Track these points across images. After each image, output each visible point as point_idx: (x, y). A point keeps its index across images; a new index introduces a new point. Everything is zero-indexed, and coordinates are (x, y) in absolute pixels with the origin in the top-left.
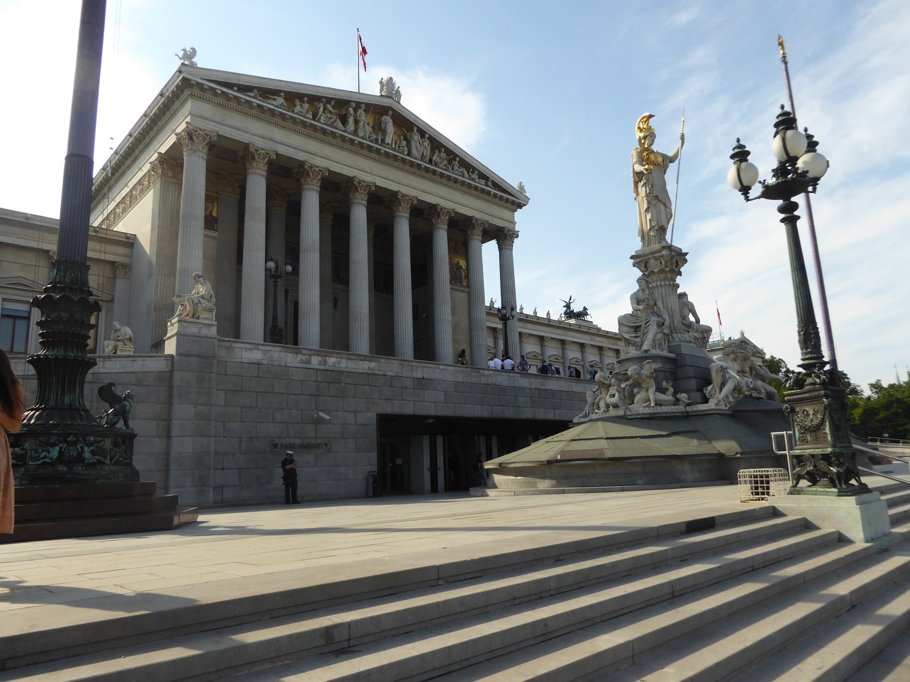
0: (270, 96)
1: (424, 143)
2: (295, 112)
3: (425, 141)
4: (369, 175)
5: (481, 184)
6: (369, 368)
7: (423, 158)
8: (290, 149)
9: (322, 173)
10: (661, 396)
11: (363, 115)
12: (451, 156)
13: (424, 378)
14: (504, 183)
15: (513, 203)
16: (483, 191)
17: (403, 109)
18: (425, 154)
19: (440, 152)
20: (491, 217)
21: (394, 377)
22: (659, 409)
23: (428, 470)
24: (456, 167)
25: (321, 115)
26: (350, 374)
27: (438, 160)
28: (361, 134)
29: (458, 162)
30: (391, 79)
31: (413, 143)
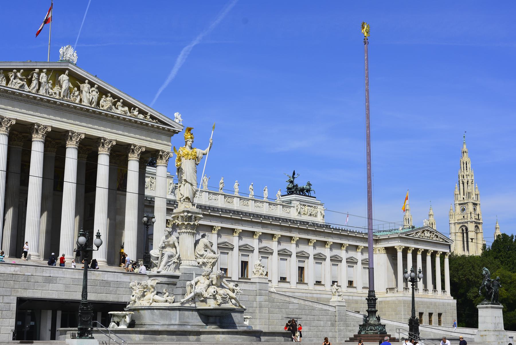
1: (93, 92)
3: (94, 91)
6: (14, 271)
7: (91, 103)
9: (11, 123)
10: (157, 297)
11: (44, 78)
12: (116, 100)
13: (50, 277)
15: (169, 130)
16: (141, 123)
18: (93, 101)
19: (107, 96)
21: (30, 276)
22: (154, 304)
23: (50, 330)
24: (120, 108)
25: (13, 81)
26: (2, 274)
27: (104, 104)
28: (42, 91)
29: (122, 103)
31: (84, 92)
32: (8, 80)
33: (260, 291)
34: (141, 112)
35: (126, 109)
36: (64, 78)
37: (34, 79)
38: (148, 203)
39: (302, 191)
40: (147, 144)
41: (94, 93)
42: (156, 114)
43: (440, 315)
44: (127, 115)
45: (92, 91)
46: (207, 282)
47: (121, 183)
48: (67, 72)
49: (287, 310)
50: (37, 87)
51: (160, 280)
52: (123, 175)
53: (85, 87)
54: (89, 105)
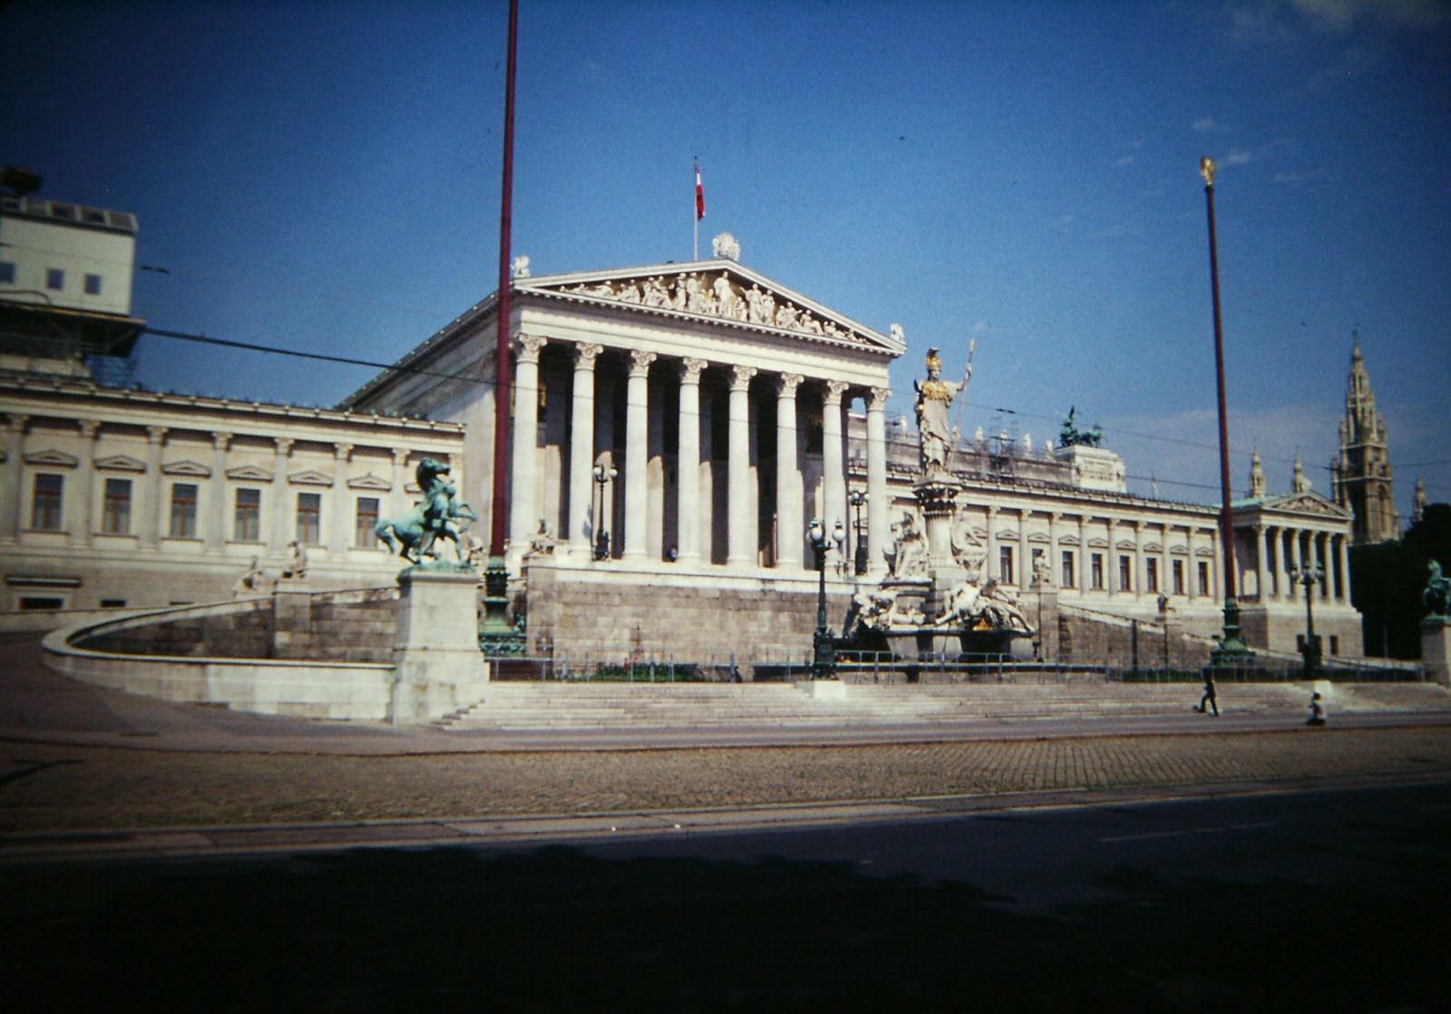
7: (764, 319)
15: (884, 354)
16: (841, 346)
24: (807, 324)
31: (752, 304)
32: (642, 294)
34: (839, 327)
35: (816, 324)
36: (722, 284)
37: (678, 289)
39: (1087, 440)
42: (862, 330)
43: (1334, 640)
48: (726, 274)
50: (684, 302)
51: (902, 589)
53: (754, 295)
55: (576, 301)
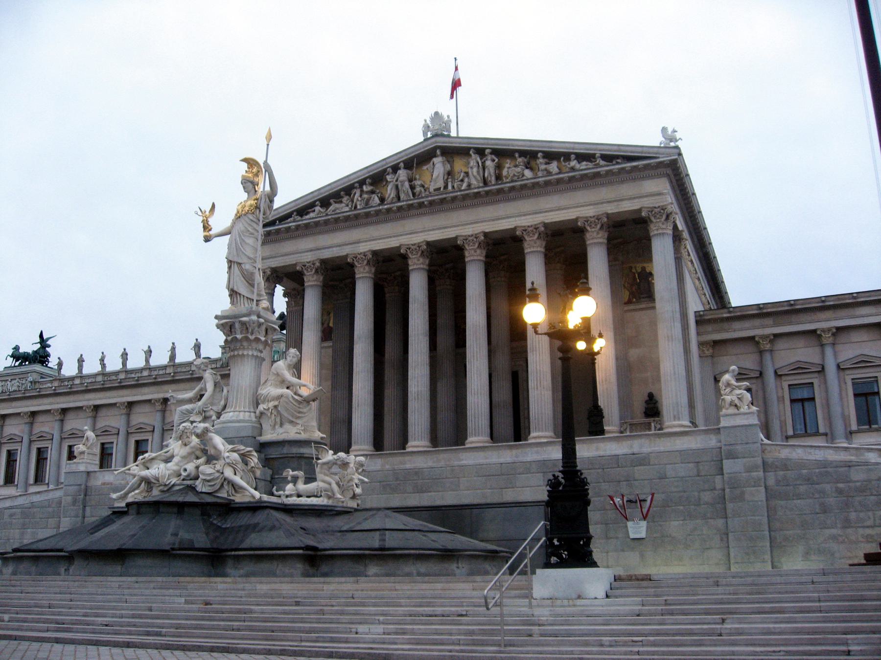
0: (310, 210)
2: (329, 213)
3: (487, 159)
4: (423, 234)
5: (584, 166)
7: (485, 182)
8: (334, 249)
14: (622, 148)
17: (451, 140)
18: (486, 175)
19: (515, 159)
20: (616, 204)
25: (358, 200)
28: (402, 196)
29: (544, 157)
30: (436, 113)
33: (727, 447)
38: (757, 310)
40: (613, 208)
41: (489, 163)
44: (554, 173)
45: (483, 163)
46: (185, 451)
47: (634, 290)
48: (438, 152)
49: (841, 485)
52: (637, 275)
53: (475, 159)
54: (481, 185)
55: (288, 229)
